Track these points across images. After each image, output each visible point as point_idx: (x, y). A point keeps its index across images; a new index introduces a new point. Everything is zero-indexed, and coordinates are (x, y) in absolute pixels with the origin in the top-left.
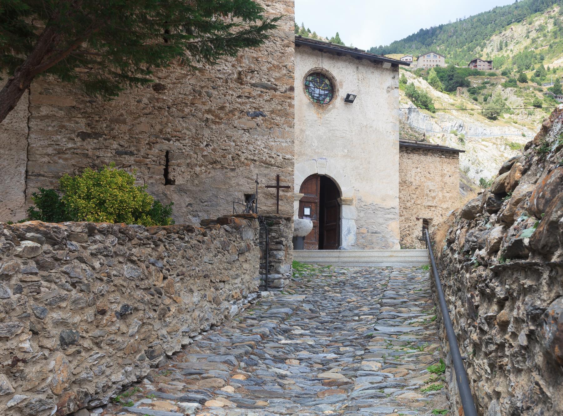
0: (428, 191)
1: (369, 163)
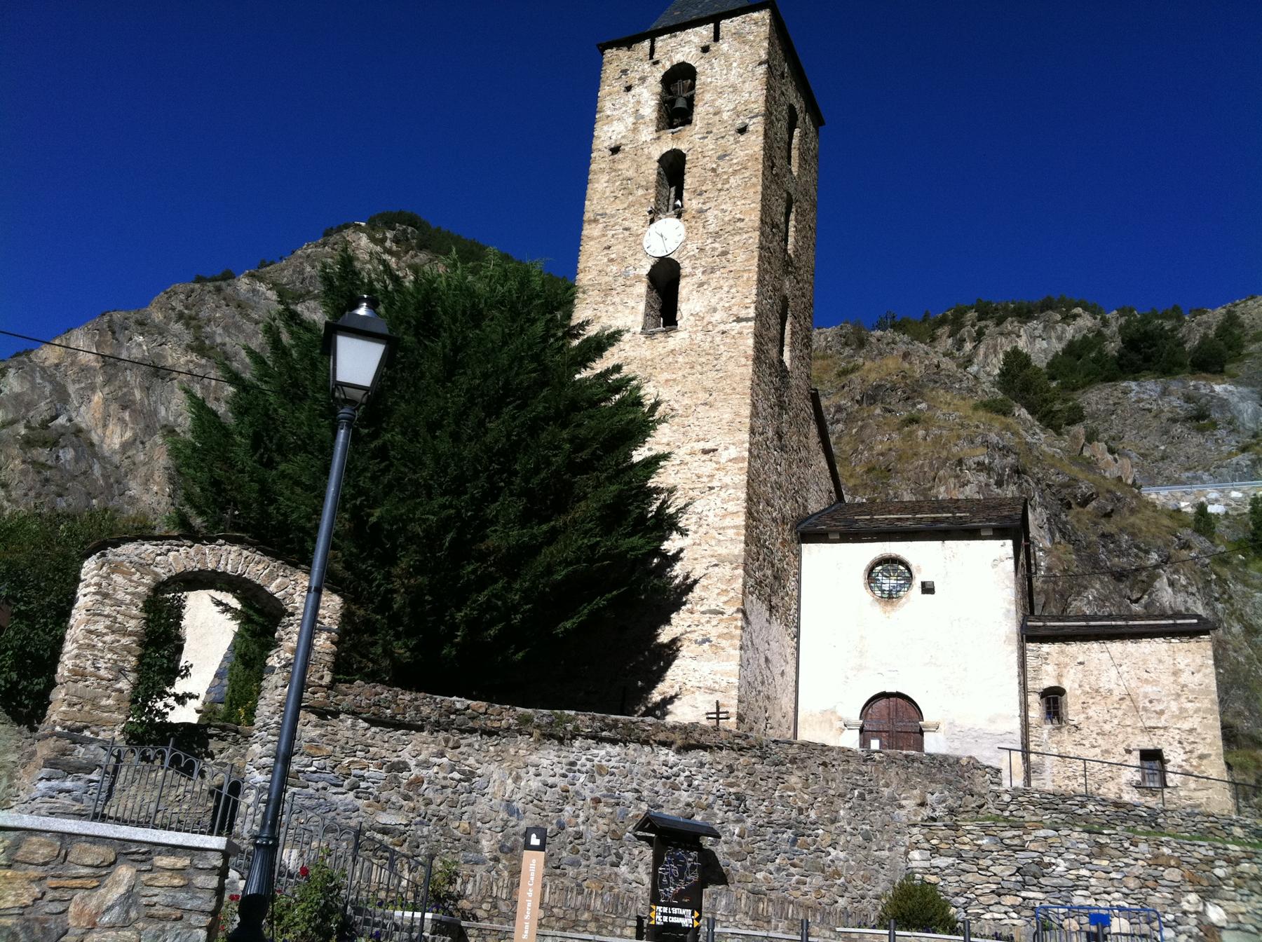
0: (1146, 701)
1: (965, 670)
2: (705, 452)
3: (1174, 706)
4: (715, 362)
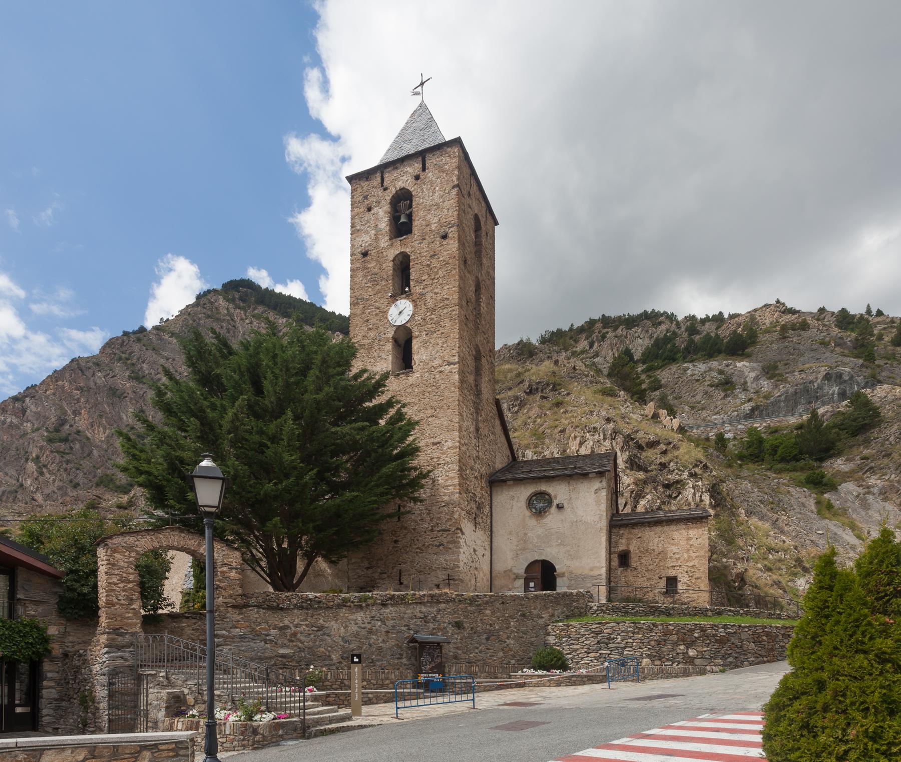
2: (434, 444)
3: (686, 555)
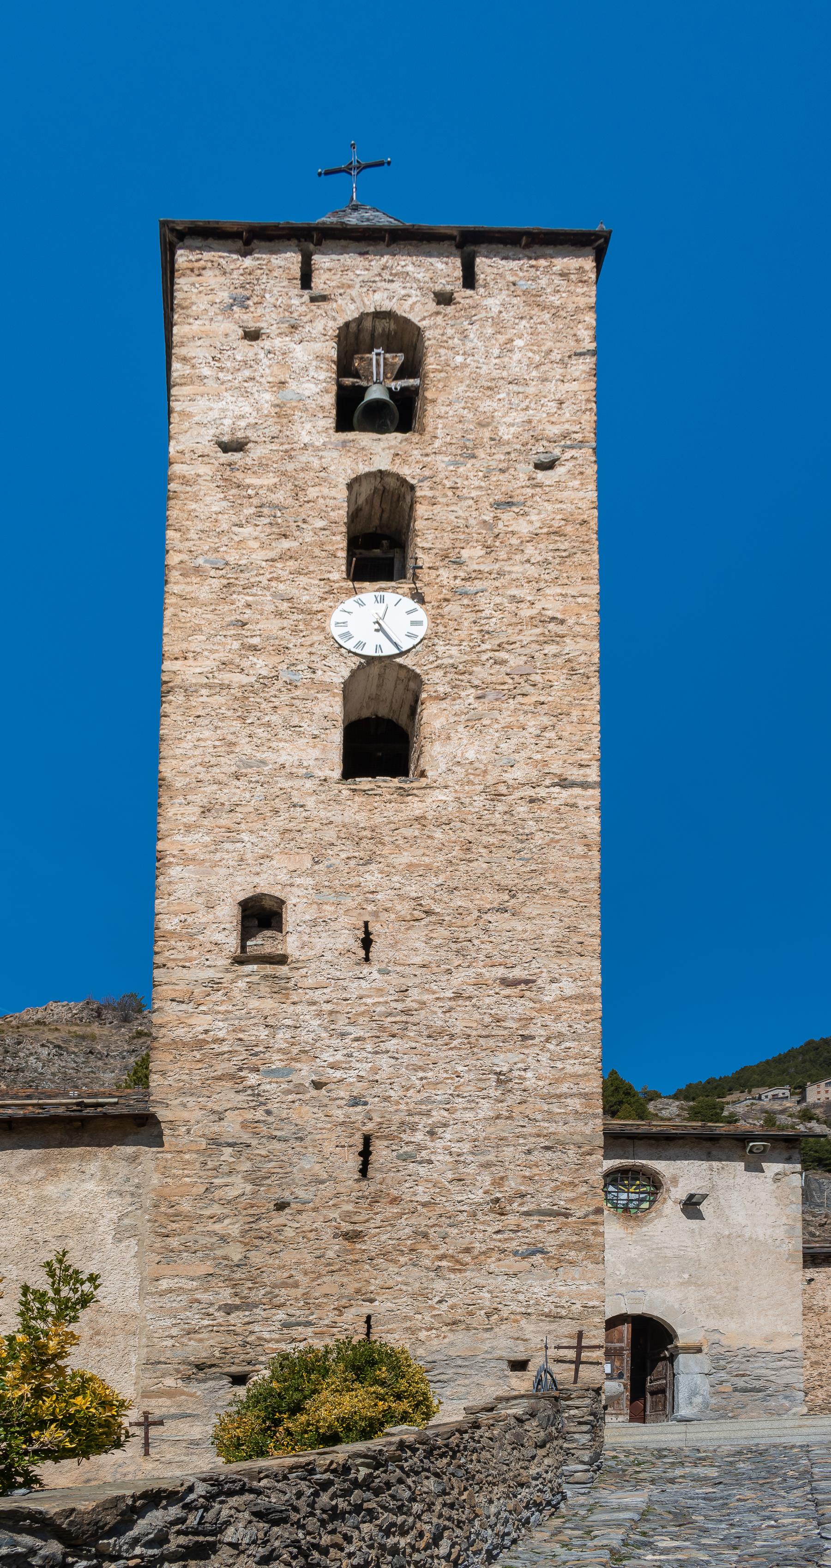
4: (520, 846)
